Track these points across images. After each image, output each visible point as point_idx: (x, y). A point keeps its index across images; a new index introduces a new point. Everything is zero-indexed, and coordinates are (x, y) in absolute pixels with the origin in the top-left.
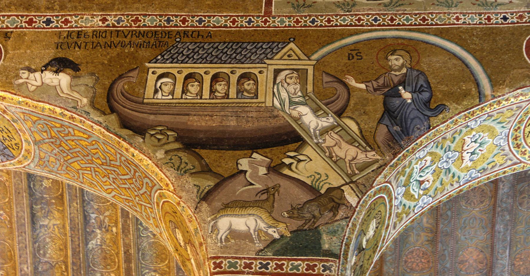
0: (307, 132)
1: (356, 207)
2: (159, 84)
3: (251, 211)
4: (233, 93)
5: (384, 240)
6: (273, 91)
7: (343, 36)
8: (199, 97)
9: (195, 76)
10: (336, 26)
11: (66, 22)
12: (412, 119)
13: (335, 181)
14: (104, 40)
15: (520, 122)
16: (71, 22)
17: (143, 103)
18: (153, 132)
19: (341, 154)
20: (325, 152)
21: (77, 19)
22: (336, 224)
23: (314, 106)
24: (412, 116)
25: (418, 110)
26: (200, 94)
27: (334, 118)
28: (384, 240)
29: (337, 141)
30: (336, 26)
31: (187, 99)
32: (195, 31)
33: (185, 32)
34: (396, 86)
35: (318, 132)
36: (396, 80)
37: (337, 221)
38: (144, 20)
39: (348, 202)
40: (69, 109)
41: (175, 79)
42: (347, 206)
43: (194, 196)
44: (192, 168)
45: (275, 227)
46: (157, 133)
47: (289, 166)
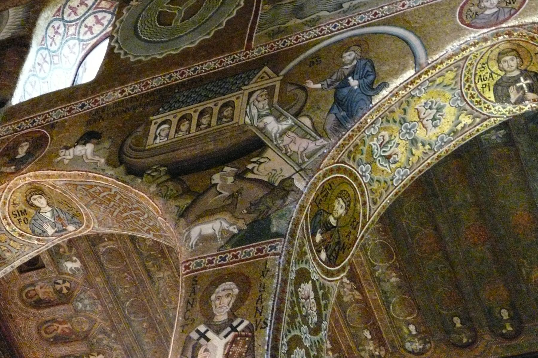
2: (158, 131)
3: (218, 216)
4: (214, 122)
5: (364, 216)
6: (246, 111)
8: (187, 133)
12: (357, 102)
13: (288, 171)
15: (467, 81)
17: (145, 150)
18: (149, 172)
22: (286, 207)
25: (363, 93)
26: (189, 131)
29: (293, 138)
34: (346, 78)
35: (278, 135)
36: (346, 72)
37: (286, 206)
38: (152, 83)
39: (297, 188)
40: (90, 170)
42: (295, 192)
43: (174, 215)
45: (236, 225)
47: (252, 171)
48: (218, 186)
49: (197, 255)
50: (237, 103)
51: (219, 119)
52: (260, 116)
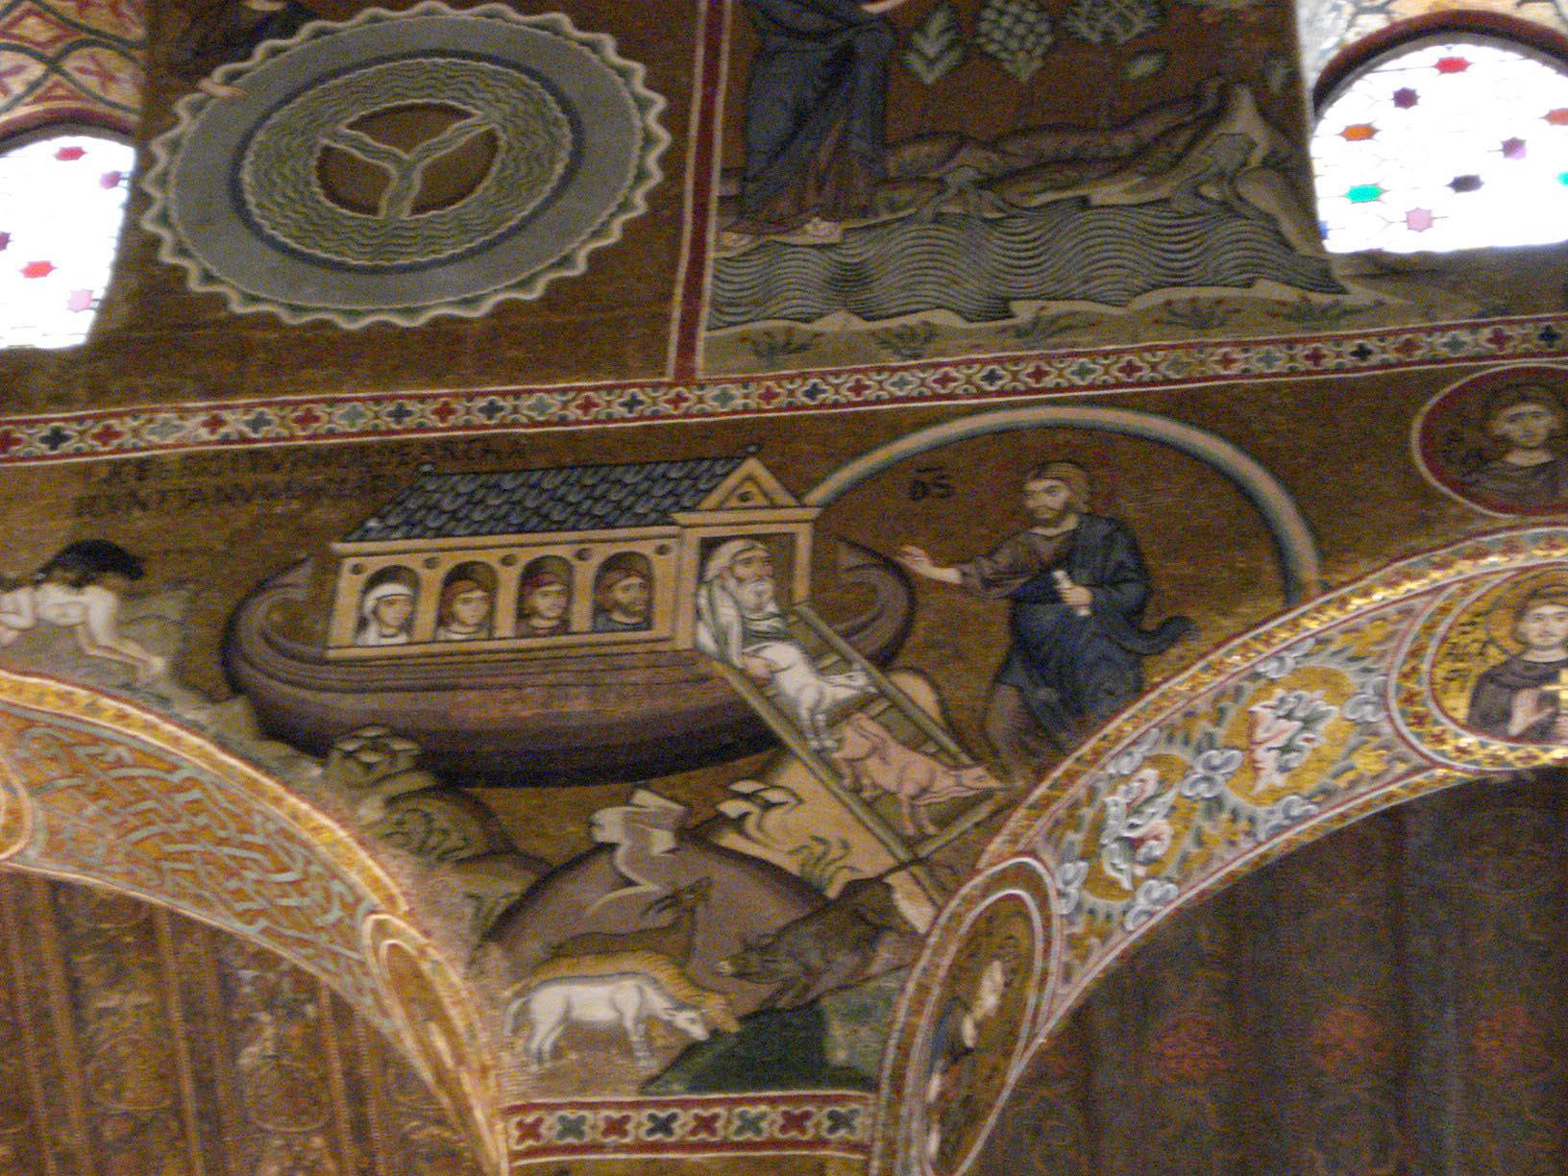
0: (790, 719)
1: (928, 935)
2: (370, 602)
3: (627, 963)
4: (581, 614)
5: (1035, 1016)
7: (897, 427)
8: (484, 634)
9: (472, 571)
10: (879, 401)
11: (107, 435)
13: (869, 858)
14: (215, 481)
16: (117, 435)
17: (325, 662)
18: (350, 746)
19: (887, 779)
20: (838, 776)
21: (135, 424)
22: (872, 985)
23: (813, 641)
24: (1090, 656)
27: (869, 675)
28: (1035, 1016)
30: (879, 401)
31: (448, 641)
32: (478, 439)
33: (447, 445)
34: (1047, 569)
35: (820, 717)
36: (1047, 550)
37: (875, 977)
39: (906, 923)
41: (414, 582)
43: (465, 927)
44: (461, 844)
46: (361, 749)
48: (620, 854)
49: (562, 1093)
50: (661, 566)
51: (600, 610)
52: (751, 636)
